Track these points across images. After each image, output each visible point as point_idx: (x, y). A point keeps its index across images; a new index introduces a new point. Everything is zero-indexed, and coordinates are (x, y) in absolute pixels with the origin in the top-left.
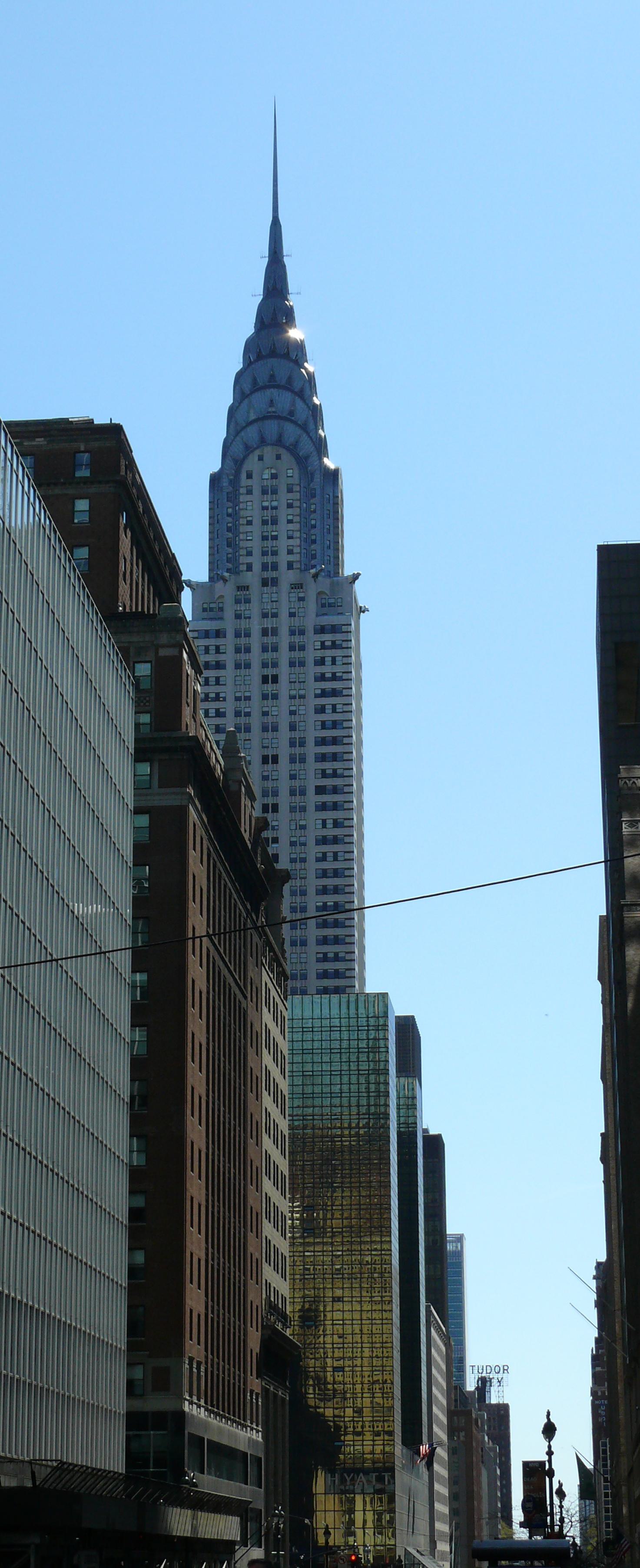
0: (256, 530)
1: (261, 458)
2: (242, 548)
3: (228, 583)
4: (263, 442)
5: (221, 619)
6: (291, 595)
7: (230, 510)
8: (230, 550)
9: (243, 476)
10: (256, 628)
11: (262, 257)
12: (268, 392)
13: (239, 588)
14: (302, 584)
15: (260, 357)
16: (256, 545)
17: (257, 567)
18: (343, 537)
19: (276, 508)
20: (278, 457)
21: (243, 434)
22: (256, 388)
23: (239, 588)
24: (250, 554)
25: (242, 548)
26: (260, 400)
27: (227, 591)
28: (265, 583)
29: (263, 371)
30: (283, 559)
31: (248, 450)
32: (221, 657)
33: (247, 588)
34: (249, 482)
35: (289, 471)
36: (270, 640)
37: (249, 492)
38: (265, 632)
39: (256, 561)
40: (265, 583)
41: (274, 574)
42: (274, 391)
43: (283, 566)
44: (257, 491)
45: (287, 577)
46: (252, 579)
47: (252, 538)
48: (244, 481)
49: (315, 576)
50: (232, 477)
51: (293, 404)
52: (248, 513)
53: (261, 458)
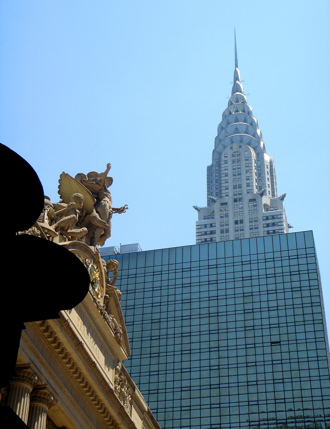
1: (231, 148)
2: (223, 187)
3: (216, 203)
4: (232, 142)
5: (213, 218)
6: (249, 205)
7: (217, 174)
8: (217, 184)
9: (223, 157)
10: (231, 221)
11: (231, 83)
13: (222, 204)
14: (255, 199)
16: (230, 185)
17: (231, 194)
18: (276, 185)
19: (240, 168)
20: (240, 147)
21: (222, 142)
23: (222, 204)
24: (227, 189)
25: (223, 187)
27: (217, 206)
28: (235, 201)
30: (245, 188)
31: (225, 147)
33: (226, 204)
34: (226, 159)
35: (246, 152)
36: (239, 225)
37: (226, 162)
38: (236, 222)
39: (231, 192)
40: (235, 201)
41: (240, 196)
43: (245, 192)
44: (230, 162)
45: (246, 197)
46: (229, 200)
47: (229, 181)
48: (223, 158)
50: (217, 161)
53: (231, 148)
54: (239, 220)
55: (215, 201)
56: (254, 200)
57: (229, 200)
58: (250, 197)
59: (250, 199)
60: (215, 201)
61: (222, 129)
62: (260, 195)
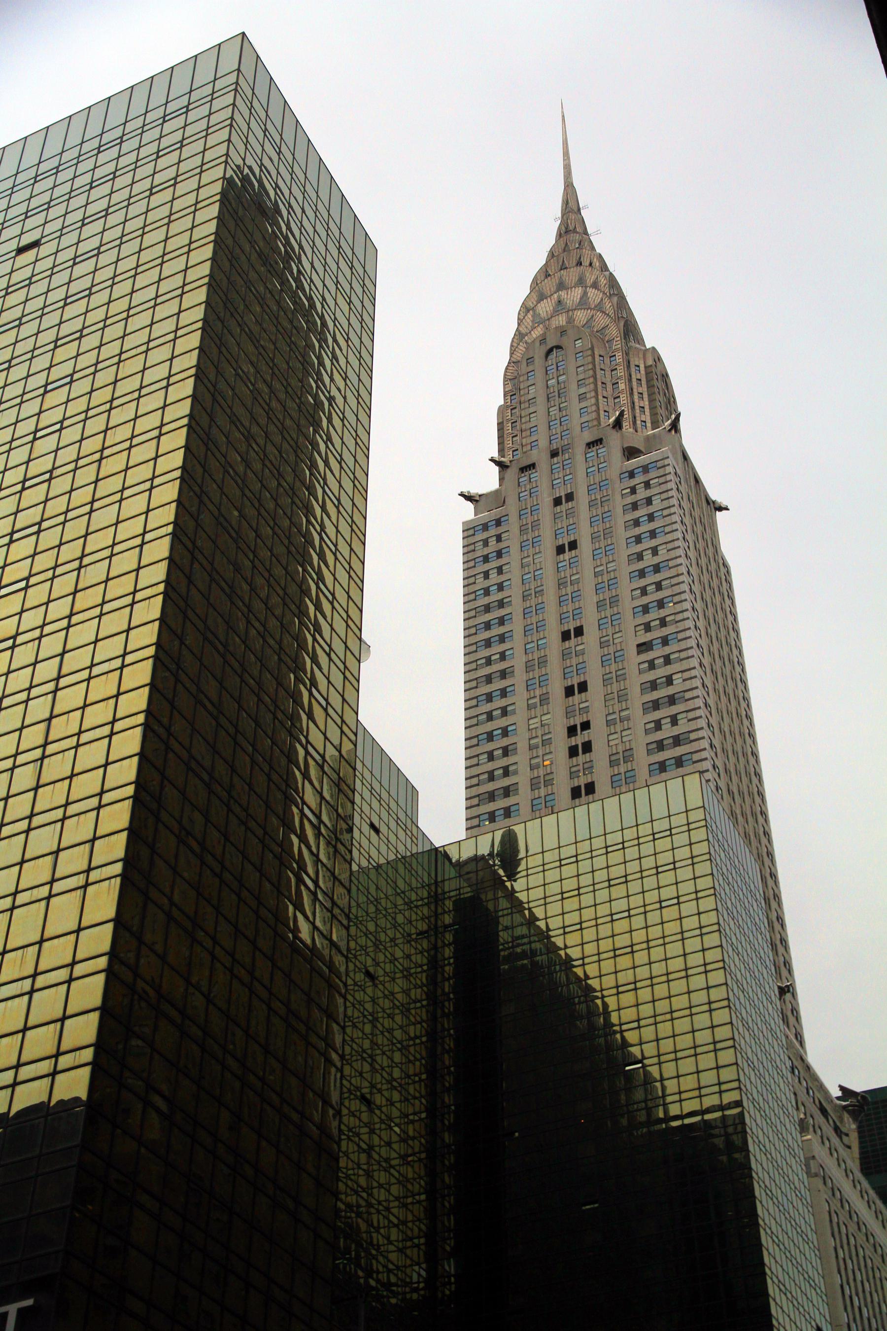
0: (541, 406)
3: (509, 471)
12: (556, 296)
13: (523, 470)
15: (547, 275)
22: (542, 297)
23: (523, 470)
26: (545, 308)
29: (549, 285)
30: (576, 421)
32: (502, 545)
33: (533, 466)
42: (563, 293)
44: (539, 374)
49: (618, 424)
51: (585, 293)
52: (530, 396)
54: (563, 494)
55: (507, 467)
56: (599, 441)
57: (539, 455)
58: (588, 437)
59: (589, 440)
60: (507, 467)
61: (528, 311)
62: (614, 427)
